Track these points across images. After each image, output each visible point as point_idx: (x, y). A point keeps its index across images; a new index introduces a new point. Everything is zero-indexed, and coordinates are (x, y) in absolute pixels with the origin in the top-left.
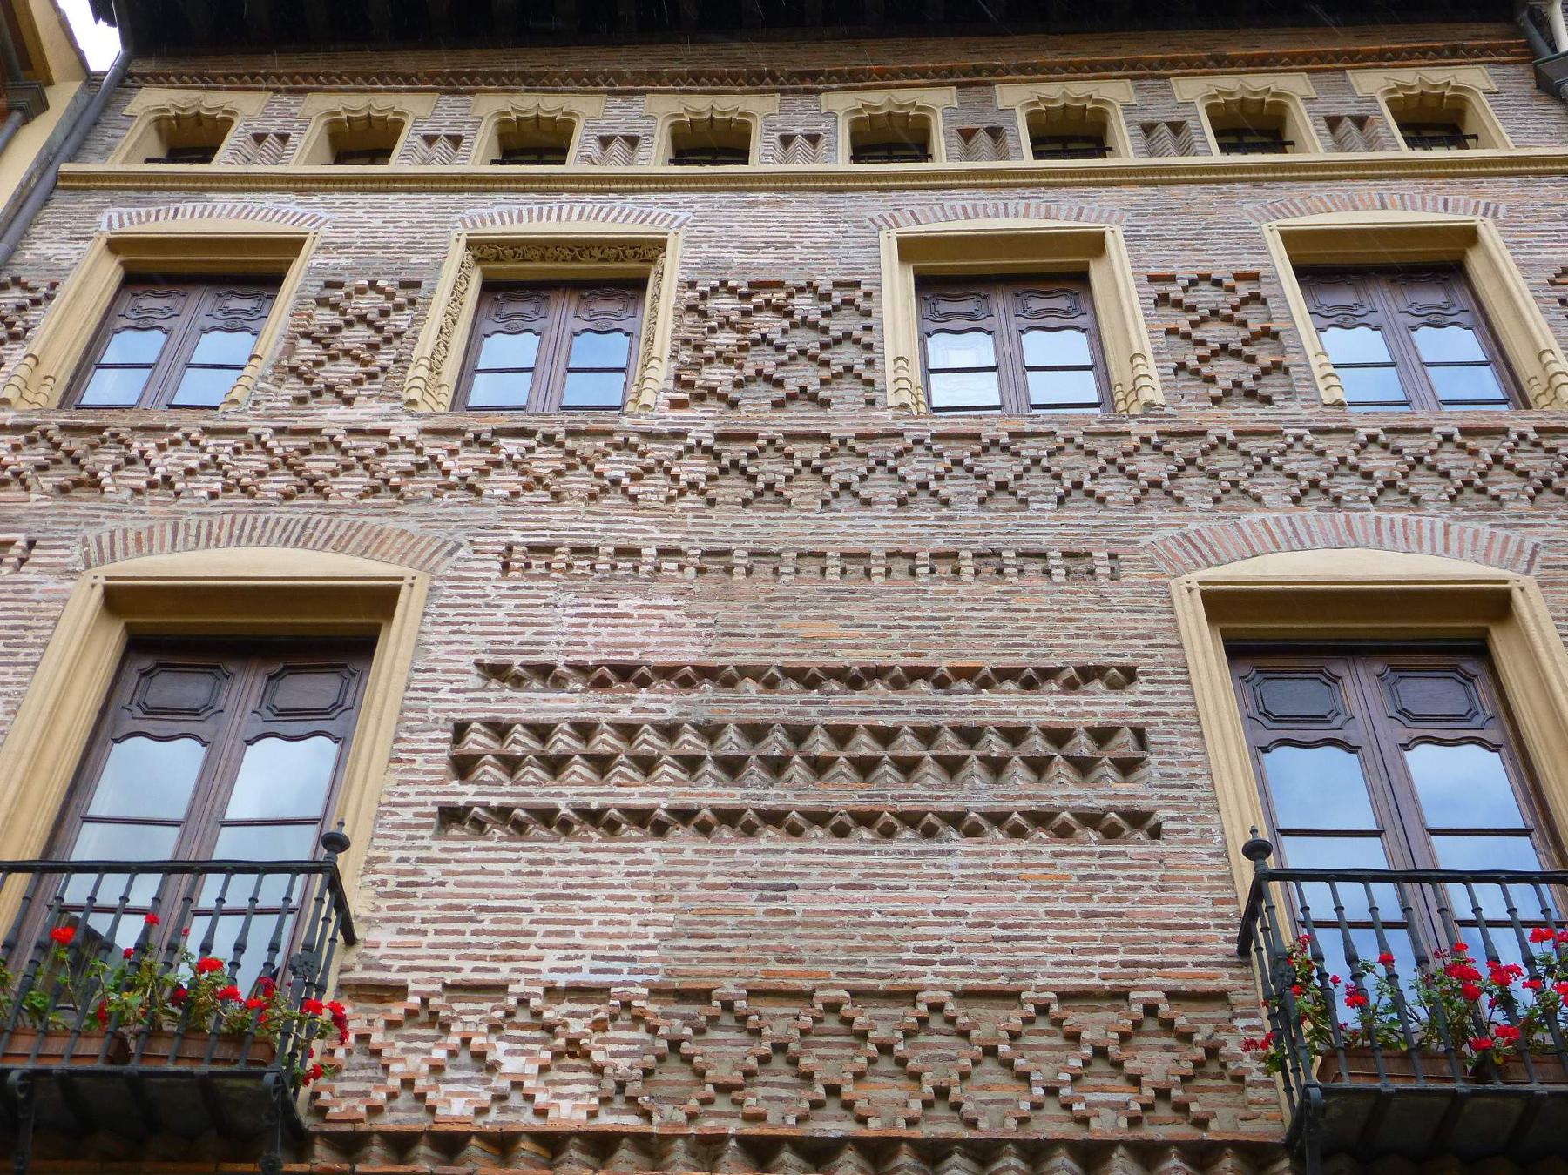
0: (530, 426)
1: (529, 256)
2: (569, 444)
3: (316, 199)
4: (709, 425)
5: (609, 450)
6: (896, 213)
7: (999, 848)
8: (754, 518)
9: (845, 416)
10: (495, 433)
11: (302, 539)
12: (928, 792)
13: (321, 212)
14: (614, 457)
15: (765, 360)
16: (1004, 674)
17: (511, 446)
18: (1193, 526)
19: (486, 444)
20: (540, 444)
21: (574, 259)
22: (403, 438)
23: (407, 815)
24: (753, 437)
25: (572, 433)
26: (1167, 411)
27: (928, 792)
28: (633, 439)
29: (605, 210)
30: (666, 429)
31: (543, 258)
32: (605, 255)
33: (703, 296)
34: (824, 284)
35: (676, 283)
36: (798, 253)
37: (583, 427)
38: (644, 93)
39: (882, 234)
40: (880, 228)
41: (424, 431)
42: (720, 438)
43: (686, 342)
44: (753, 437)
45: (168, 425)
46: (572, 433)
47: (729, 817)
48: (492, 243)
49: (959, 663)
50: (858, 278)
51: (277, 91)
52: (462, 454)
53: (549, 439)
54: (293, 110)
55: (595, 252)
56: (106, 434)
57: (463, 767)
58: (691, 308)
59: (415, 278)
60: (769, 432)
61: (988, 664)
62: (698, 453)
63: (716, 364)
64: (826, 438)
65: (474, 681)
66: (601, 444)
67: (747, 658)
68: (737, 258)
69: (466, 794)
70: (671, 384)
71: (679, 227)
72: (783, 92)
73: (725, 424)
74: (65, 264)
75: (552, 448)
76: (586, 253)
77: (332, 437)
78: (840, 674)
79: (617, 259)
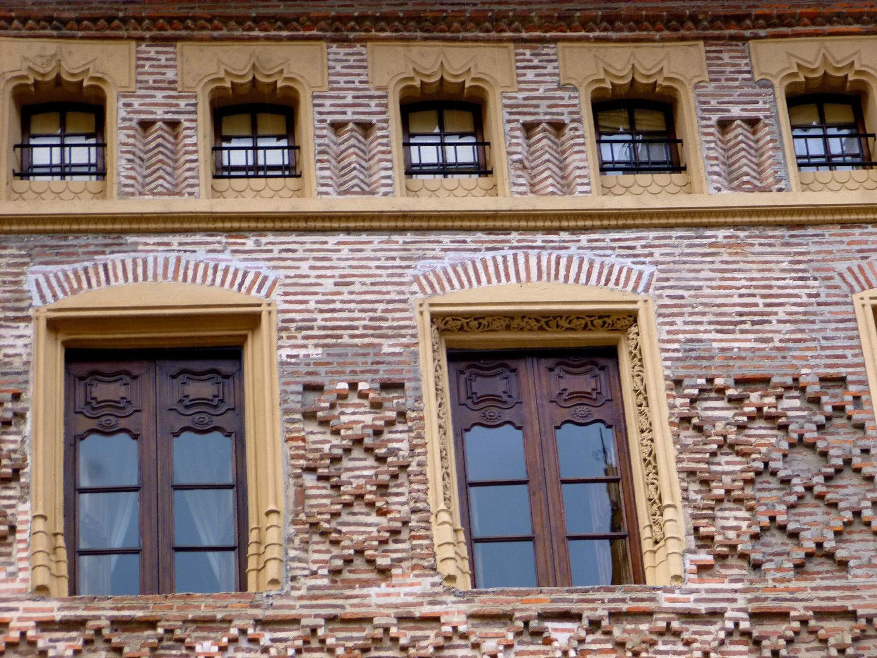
0: (575, 608)
1: (494, 327)
2: (617, 633)
3: (250, 243)
4: (741, 603)
5: (654, 637)
6: (864, 263)
10: (544, 616)
13: (264, 268)
14: (660, 647)
15: (771, 499)
19: (537, 634)
20: (588, 632)
21: (541, 329)
22: (455, 628)
24: (784, 616)
25: (616, 616)
28: (675, 625)
29: (563, 262)
30: (703, 608)
31: (508, 328)
32: (572, 325)
33: (693, 400)
34: (809, 376)
35: (662, 384)
36: (779, 331)
37: (624, 607)
38: (555, 40)
39: (856, 298)
40: (853, 291)
41: (471, 616)
42: (757, 616)
43: (691, 473)
44: (784, 616)
45: (219, 616)
46: (616, 616)
48: (455, 316)
50: (843, 371)
51: (140, 39)
52: (518, 648)
53: (595, 625)
54: (170, 74)
55: (563, 323)
56: (160, 631)
58: (685, 420)
59: (396, 378)
60: (798, 610)
62: (737, 637)
63: (727, 505)
64: (852, 615)
66: (644, 627)
68: (716, 341)
70: (692, 542)
71: (646, 290)
72: (706, 39)
73: (757, 599)
74: (17, 363)
75: (598, 635)
76: (553, 323)
77: (386, 630)
79: (585, 328)
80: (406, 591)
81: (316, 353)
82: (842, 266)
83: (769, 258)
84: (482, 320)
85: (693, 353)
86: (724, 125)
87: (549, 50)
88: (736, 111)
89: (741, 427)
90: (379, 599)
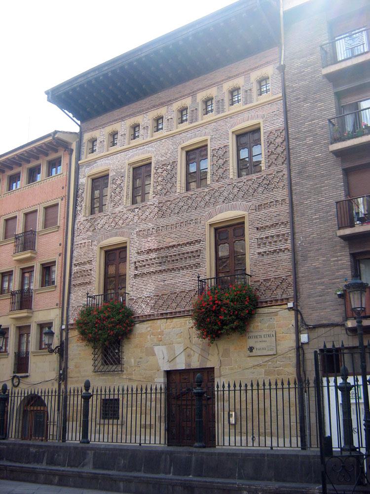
3: (109, 158)
7: (185, 271)
8: (162, 220)
9: (172, 196)
10: (134, 209)
11: (116, 235)
12: (178, 265)
16: (188, 243)
17: (136, 210)
18: (210, 210)
23: (132, 276)
25: (142, 207)
26: (211, 185)
27: (178, 265)
36: (169, 155)
47: (160, 271)
49: (183, 242)
57: (136, 268)
61: (185, 242)
65: (136, 255)
67: (161, 246)
68: (160, 159)
69: (137, 272)
78: (170, 246)
80: (120, 208)
81: (114, 174)
82: (178, 142)
83: (169, 142)
84: (134, 163)
85: (158, 162)
86: (168, 120)
87: (148, 114)
88: (169, 117)
89: (162, 173)
90: (117, 210)
